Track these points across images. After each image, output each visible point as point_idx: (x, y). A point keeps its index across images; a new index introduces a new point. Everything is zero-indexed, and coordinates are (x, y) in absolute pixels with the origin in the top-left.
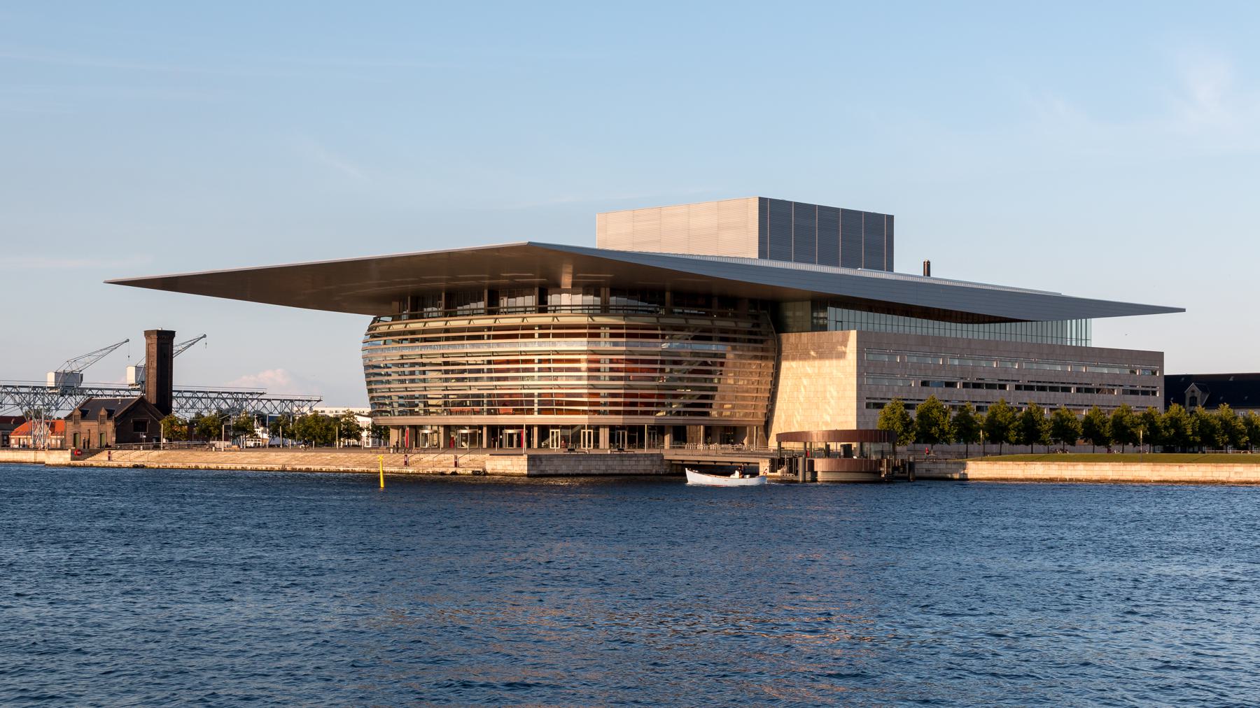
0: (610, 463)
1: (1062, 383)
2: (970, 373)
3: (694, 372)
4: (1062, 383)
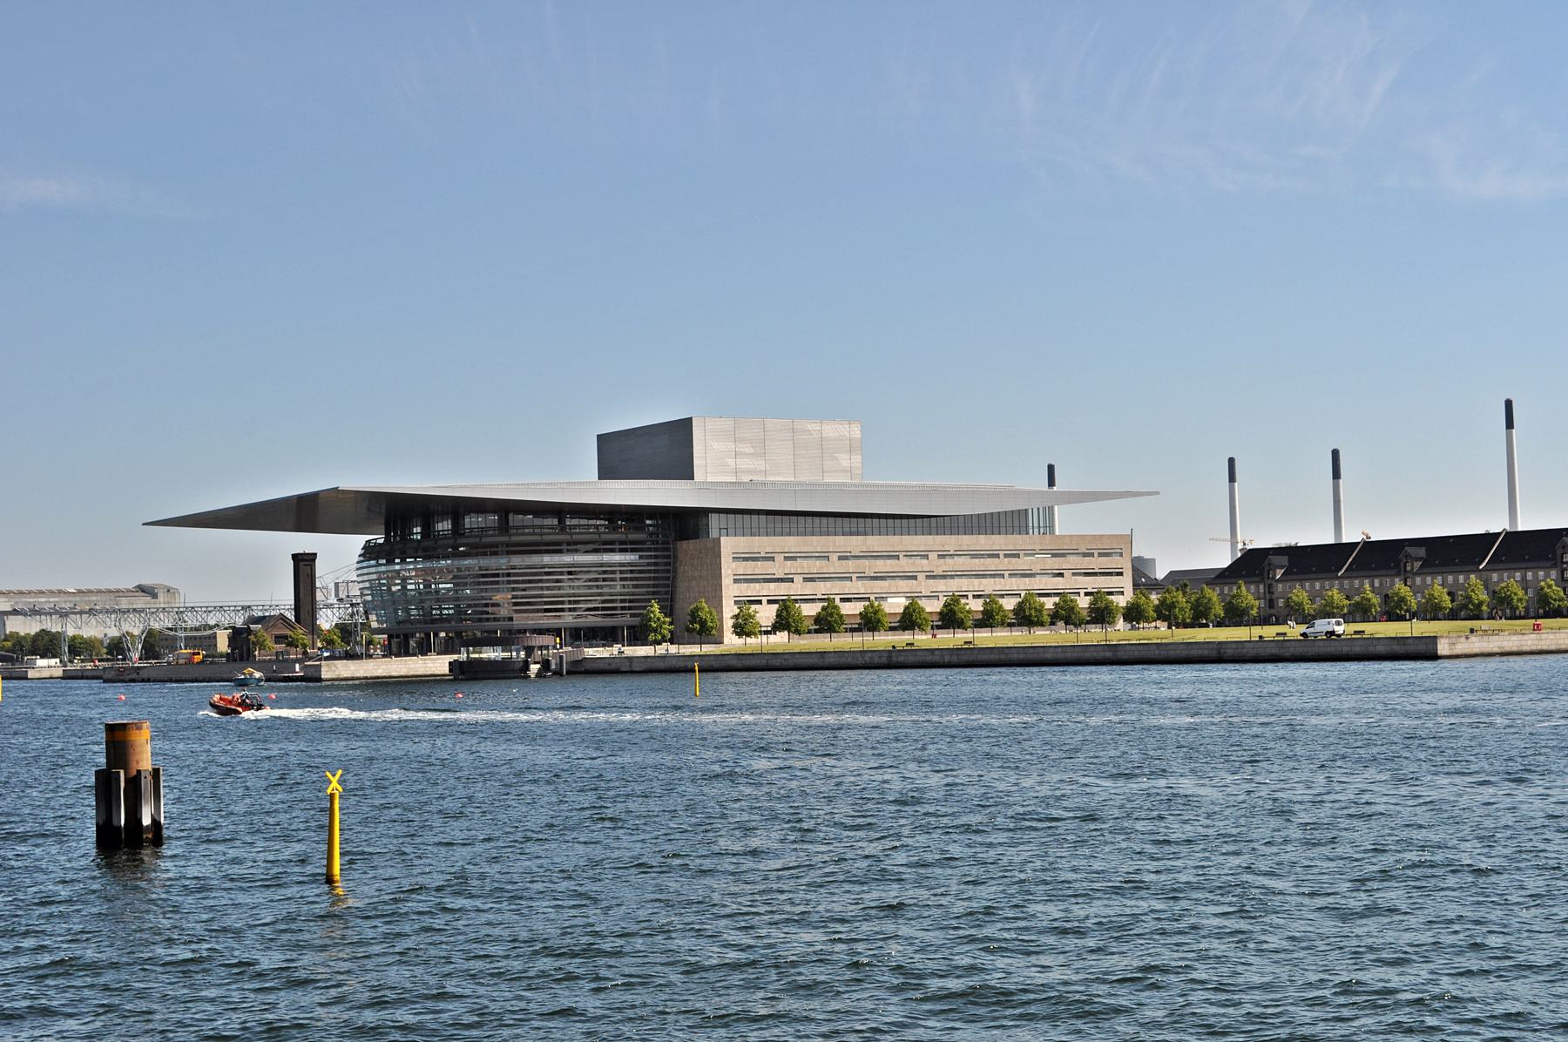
0: (412, 666)
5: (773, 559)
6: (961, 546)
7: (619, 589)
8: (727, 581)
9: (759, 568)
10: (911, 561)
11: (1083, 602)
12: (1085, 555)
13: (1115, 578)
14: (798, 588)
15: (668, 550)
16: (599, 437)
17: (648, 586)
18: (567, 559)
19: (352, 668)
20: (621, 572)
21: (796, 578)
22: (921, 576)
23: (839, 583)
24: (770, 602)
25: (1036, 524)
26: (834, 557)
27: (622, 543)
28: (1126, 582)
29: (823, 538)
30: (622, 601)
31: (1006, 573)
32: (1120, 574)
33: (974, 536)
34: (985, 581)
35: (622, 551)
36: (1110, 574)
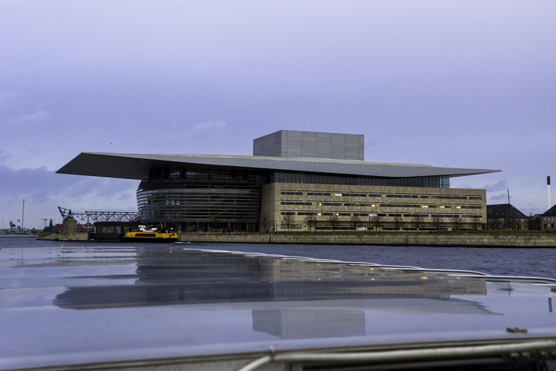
1: (413, 203)
2: (350, 200)
3: (223, 201)
4: (413, 203)
5: (301, 194)
6: (399, 191)
7: (235, 206)
8: (278, 203)
9: (295, 198)
10: (373, 198)
12: (463, 198)
13: (477, 210)
15: (257, 188)
16: (254, 140)
17: (247, 205)
18: (214, 191)
19: (77, 236)
20: (236, 198)
21: (313, 203)
23: (335, 207)
24: (299, 214)
27: (237, 184)
28: (483, 212)
29: (327, 185)
30: (236, 211)
32: (480, 208)
33: (406, 187)
34: (410, 208)
35: (237, 188)
36: (475, 208)
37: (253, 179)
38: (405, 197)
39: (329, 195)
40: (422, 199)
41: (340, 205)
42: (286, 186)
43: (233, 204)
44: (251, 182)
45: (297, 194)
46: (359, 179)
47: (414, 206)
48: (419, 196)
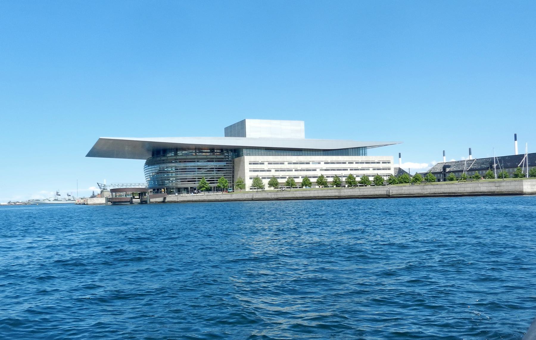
5: (263, 164)
11: (371, 179)
14: (273, 173)
15: (231, 161)
18: (199, 164)
22: (318, 170)
25: (362, 153)
26: (286, 163)
31: (349, 169)
32: (389, 169)
35: (216, 161)
36: (386, 169)
37: (227, 154)
38: (338, 163)
39: (283, 163)
40: (349, 164)
41: (291, 170)
42: (253, 158)
43: (214, 173)
44: (226, 157)
45: (261, 164)
46: (303, 152)
47: (344, 170)
48: (347, 162)
